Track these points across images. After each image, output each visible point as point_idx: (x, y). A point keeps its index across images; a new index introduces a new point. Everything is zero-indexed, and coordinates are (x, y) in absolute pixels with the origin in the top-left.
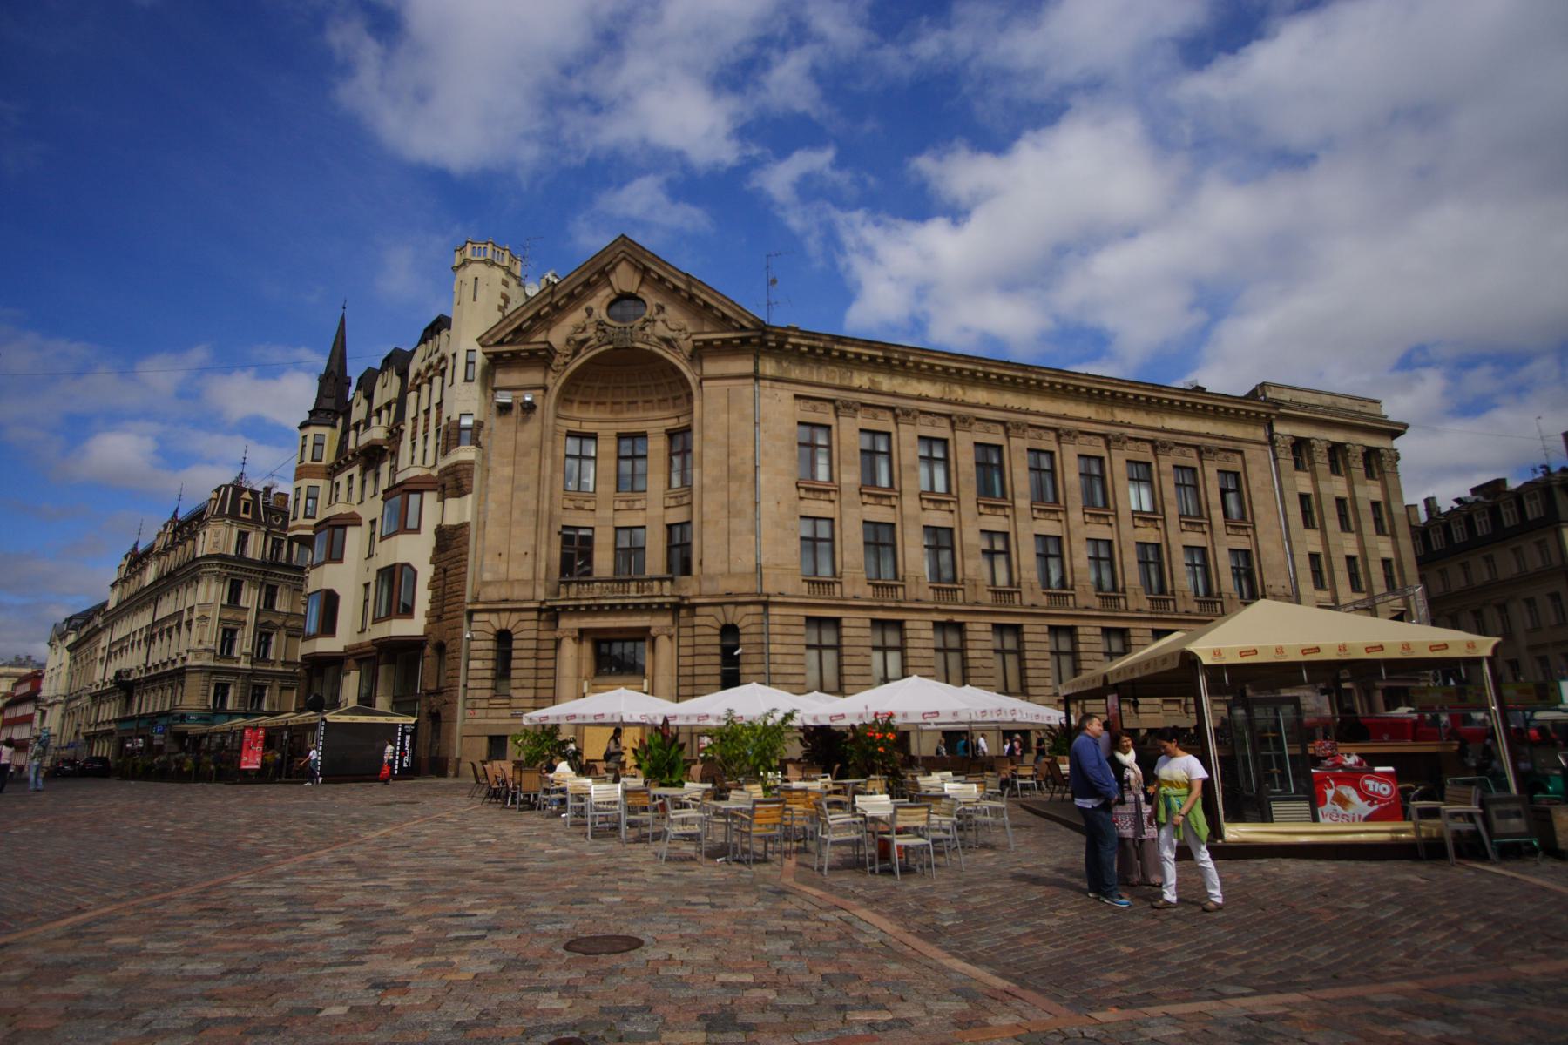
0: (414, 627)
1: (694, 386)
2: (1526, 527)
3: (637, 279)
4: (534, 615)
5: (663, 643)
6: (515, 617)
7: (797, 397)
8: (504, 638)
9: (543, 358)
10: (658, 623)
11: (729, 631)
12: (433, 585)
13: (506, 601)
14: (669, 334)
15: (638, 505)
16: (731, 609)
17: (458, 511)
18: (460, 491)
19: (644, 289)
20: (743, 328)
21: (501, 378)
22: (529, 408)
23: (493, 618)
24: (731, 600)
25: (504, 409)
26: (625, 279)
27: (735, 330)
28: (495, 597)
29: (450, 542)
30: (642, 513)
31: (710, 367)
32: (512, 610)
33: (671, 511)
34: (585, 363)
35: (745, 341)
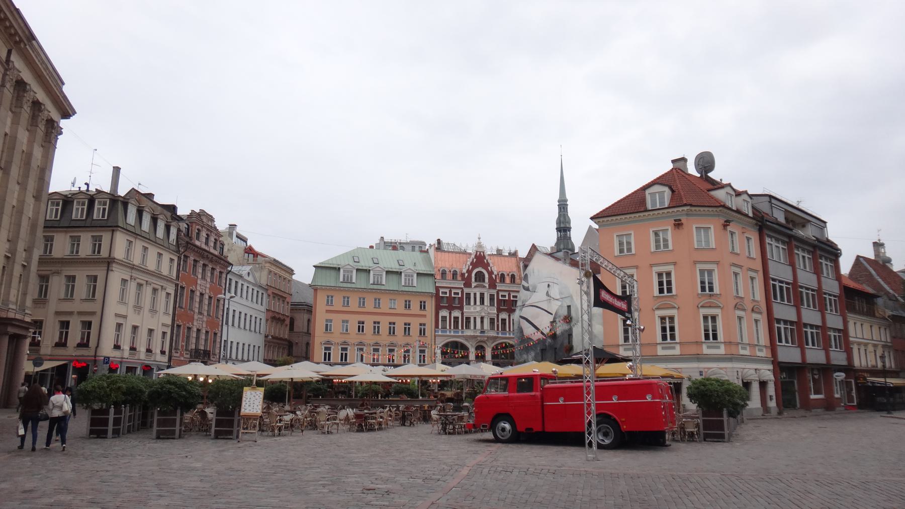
2: (87, 224)
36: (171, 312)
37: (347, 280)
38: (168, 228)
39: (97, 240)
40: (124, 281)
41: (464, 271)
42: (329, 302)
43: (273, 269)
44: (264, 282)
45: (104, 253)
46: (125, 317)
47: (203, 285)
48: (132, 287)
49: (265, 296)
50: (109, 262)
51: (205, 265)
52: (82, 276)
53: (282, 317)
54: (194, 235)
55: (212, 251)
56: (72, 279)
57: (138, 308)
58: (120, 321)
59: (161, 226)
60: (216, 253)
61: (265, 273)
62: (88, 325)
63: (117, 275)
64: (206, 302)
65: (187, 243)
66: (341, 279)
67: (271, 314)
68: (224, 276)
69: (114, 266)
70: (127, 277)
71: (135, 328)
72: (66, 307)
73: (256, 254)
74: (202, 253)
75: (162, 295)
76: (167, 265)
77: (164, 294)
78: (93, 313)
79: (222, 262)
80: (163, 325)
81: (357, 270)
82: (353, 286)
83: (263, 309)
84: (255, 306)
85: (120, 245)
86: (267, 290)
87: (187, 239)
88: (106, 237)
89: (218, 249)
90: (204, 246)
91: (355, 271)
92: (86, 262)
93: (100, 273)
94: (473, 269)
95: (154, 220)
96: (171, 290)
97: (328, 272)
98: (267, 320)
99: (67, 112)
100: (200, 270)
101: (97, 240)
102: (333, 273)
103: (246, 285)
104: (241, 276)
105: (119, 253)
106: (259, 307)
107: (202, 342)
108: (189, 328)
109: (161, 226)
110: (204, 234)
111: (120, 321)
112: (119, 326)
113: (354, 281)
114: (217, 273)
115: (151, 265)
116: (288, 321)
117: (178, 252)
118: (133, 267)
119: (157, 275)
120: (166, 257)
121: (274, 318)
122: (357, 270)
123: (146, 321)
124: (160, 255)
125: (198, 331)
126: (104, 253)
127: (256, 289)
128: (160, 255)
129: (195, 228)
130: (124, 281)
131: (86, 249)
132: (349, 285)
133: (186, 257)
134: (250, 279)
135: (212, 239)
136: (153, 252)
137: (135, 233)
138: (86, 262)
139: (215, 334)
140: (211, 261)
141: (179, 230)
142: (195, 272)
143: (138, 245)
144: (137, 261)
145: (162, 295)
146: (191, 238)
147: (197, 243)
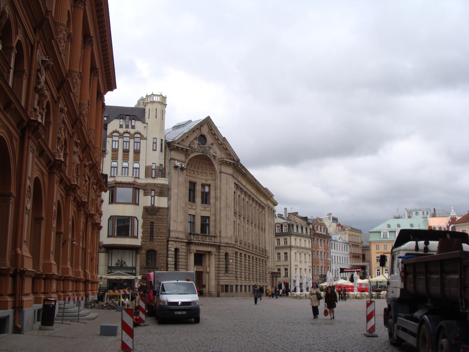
0: (137, 242)
1: (218, 173)
3: (208, 130)
4: (185, 244)
5: (213, 257)
6: (180, 244)
7: (235, 183)
8: (177, 250)
9: (186, 152)
10: (213, 250)
11: (226, 254)
12: (143, 225)
13: (177, 238)
14: (214, 154)
15: (194, 208)
16: (227, 248)
17: (161, 202)
18: (161, 194)
19: (208, 135)
20: (234, 160)
21: (174, 154)
22: (182, 169)
23: (174, 244)
24: (228, 245)
25: (176, 167)
26: (205, 131)
27: (231, 159)
28: (174, 236)
29: (150, 211)
30: (194, 211)
31: (224, 169)
32: (179, 242)
33: (202, 212)
34: (194, 157)
35: (234, 164)
36: (311, 261)
37: (385, 236)
38: (306, 229)
39: (285, 239)
40: (296, 253)
41: (445, 227)
42: (377, 248)
43: (351, 233)
44: (347, 240)
45: (288, 244)
46: (297, 266)
47: (321, 248)
48: (298, 254)
49: (348, 246)
50: (290, 247)
51: (321, 240)
52: (282, 252)
53: (357, 255)
54: (316, 229)
55: (323, 233)
56: (279, 254)
57: (301, 262)
58: (296, 267)
59: (304, 230)
60: (325, 234)
61: (347, 235)
62: (286, 269)
63: (293, 252)
64: (323, 255)
65: (314, 233)
66: (382, 237)
67: (352, 255)
68: (329, 242)
69: (292, 249)
70: (296, 251)
71: (301, 269)
72: (278, 263)
73: (342, 227)
74: (319, 235)
75: (307, 255)
76: (306, 243)
77: (308, 255)
78: (287, 265)
79: (327, 237)
80: (309, 267)
81: (389, 232)
82: (388, 240)
83: (348, 253)
84: (344, 252)
85: (293, 241)
86: (349, 244)
87: (313, 232)
88: (288, 238)
89: (325, 231)
90: (320, 232)
91: (388, 233)
92: (283, 248)
93: (288, 251)
94: (450, 225)
95: (302, 228)
96: (310, 253)
97: (375, 234)
98: (350, 258)
99: (275, 204)
100: (320, 243)
101: (285, 239)
102: (378, 234)
103: (338, 244)
104: (336, 241)
105: (293, 244)
106: (346, 252)
107: (323, 271)
108: (318, 266)
109: (304, 230)
110: (319, 227)
111: (296, 267)
112: (296, 269)
113: (388, 237)
114: (326, 242)
115: (303, 245)
116: (361, 257)
117: (311, 238)
118: (297, 247)
119: (305, 248)
120: (307, 240)
121: (353, 256)
122: (389, 232)
123: (303, 266)
124: (305, 240)
125: (322, 267)
126: (288, 244)
127: (343, 245)
128: (305, 240)
129: (315, 226)
130: (296, 253)
131: (282, 243)
132: (386, 240)
133: (314, 238)
134: (340, 241)
135: (323, 228)
136: (303, 240)
137: (297, 235)
138: (283, 248)
139: (328, 267)
140: (323, 238)
141: (310, 229)
142: (318, 243)
143: (298, 239)
144: (298, 245)
145: (307, 255)
146: (315, 231)
147: (317, 232)
